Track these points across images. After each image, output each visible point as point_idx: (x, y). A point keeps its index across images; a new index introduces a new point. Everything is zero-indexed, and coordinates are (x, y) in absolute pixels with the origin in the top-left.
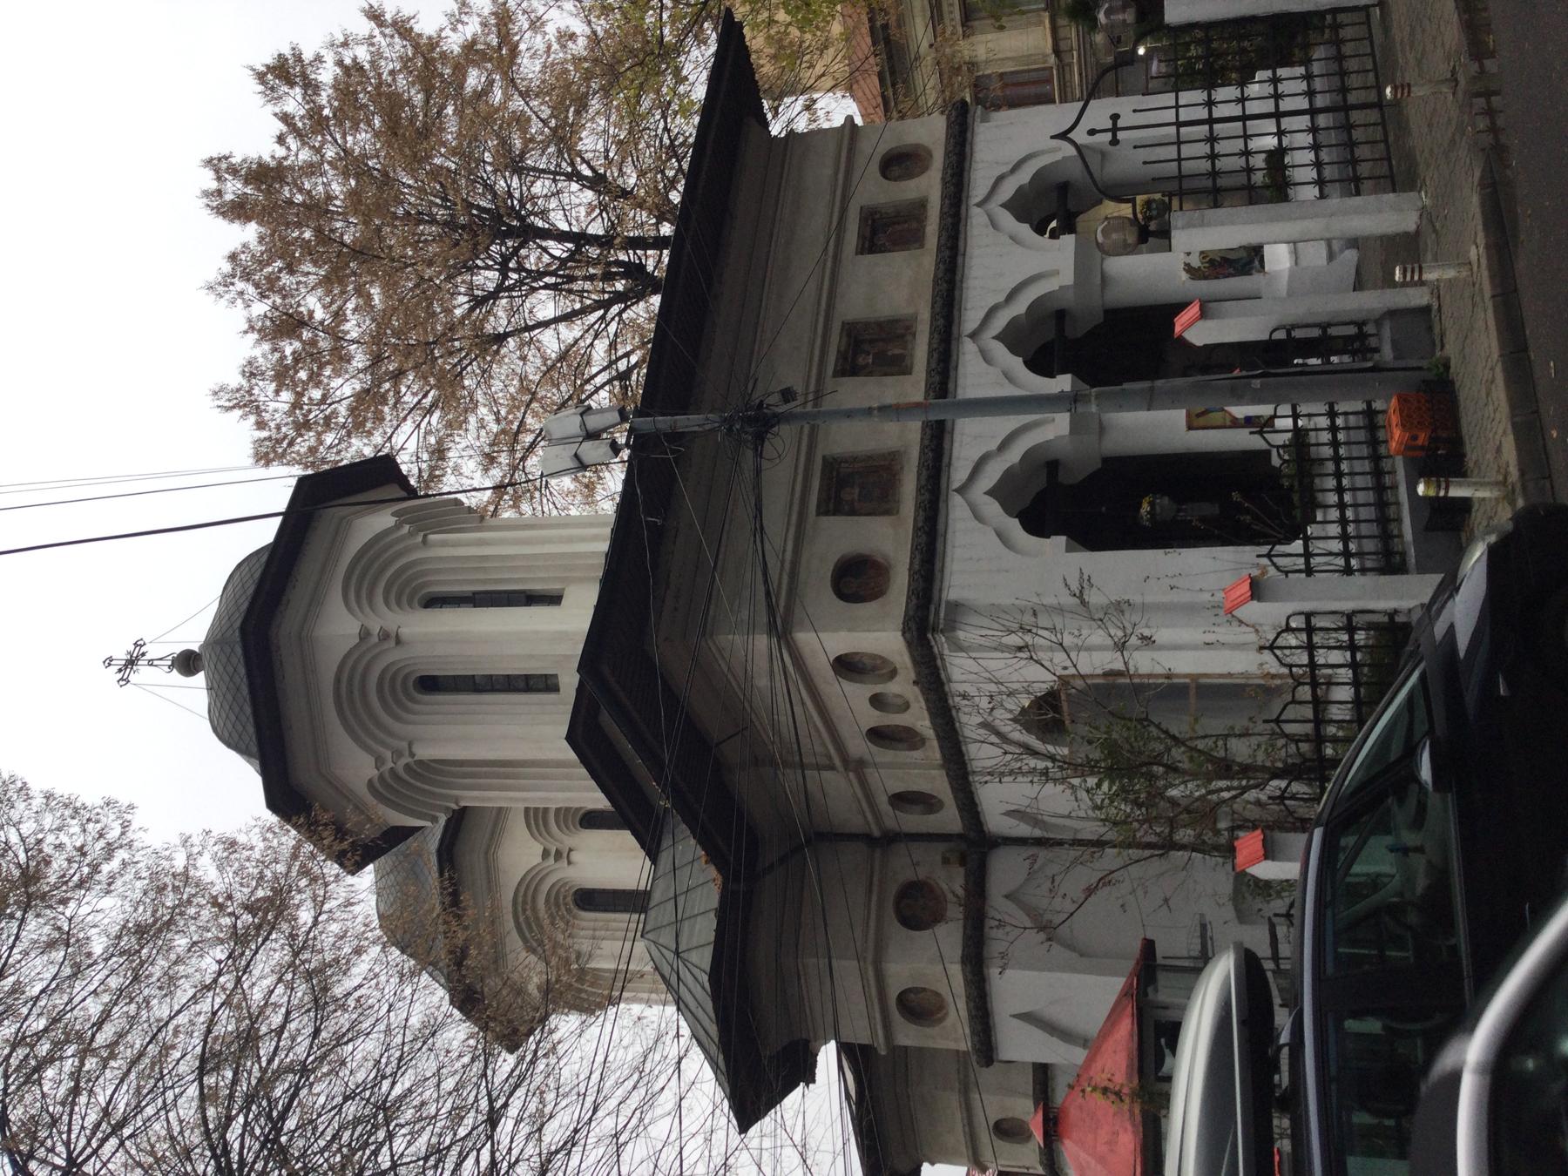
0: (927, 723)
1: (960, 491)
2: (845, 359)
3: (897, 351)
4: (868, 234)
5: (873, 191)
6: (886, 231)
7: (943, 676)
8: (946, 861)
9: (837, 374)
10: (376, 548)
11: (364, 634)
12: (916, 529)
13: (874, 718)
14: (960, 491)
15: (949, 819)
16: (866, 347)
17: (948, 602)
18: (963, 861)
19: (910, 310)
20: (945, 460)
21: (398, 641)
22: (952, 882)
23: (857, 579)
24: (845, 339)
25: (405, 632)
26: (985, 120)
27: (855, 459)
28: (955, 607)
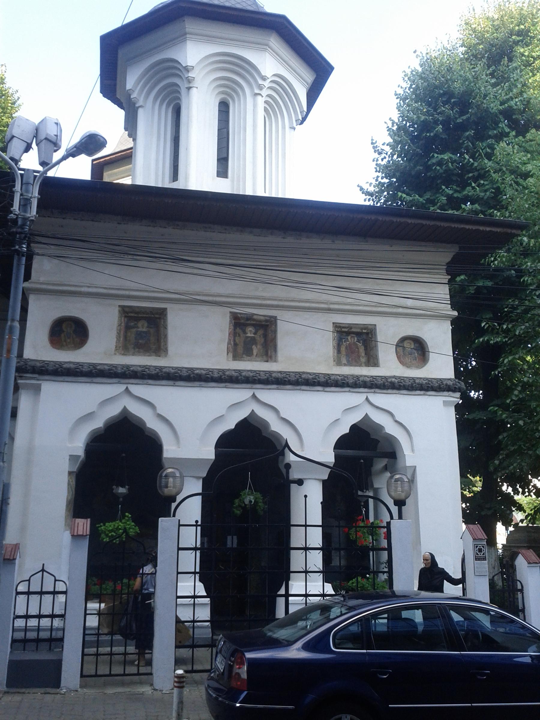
2: (248, 319)
3: (255, 352)
4: (353, 330)
5: (389, 332)
6: (357, 342)
10: (247, 66)
11: (187, 69)
16: (261, 332)
17: (40, 385)
20: (150, 381)
21: (189, 88)
24: (262, 318)
25: (194, 91)
26: (445, 403)
27: (166, 328)
28: (37, 389)
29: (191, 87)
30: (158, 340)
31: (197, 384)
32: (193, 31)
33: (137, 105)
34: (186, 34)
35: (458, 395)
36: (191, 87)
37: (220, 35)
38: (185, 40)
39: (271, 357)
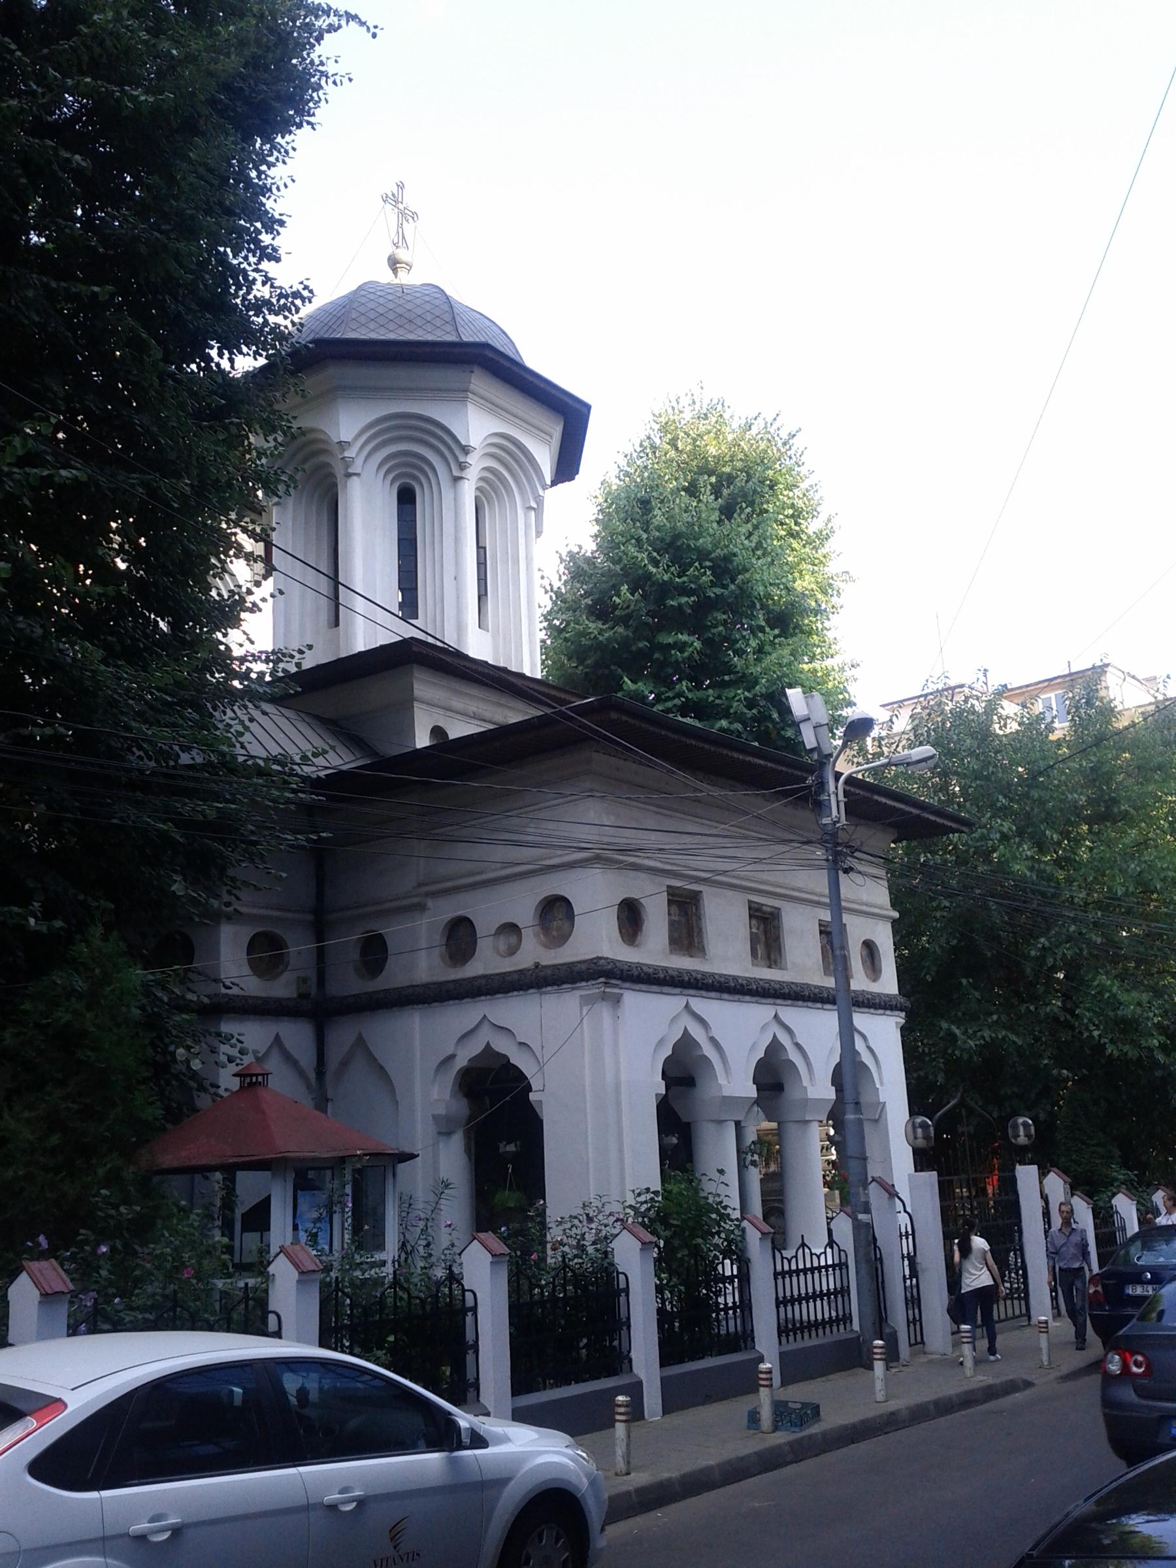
0: (481, 972)
1: (687, 1006)
7: (549, 988)
8: (304, 980)
9: (750, 902)
11: (466, 450)
12: (665, 969)
13: (485, 924)
14: (687, 1006)
15: (348, 982)
18: (303, 996)
19: (789, 966)
20: (704, 993)
22: (282, 988)
23: (630, 917)
24: (769, 909)
28: (617, 1000)
29: (462, 478)
30: (690, 935)
31: (737, 997)
32: (482, 392)
33: (350, 471)
34: (467, 390)
35: (903, 1014)
36: (462, 478)
37: (515, 410)
38: (464, 400)
39: (775, 962)
